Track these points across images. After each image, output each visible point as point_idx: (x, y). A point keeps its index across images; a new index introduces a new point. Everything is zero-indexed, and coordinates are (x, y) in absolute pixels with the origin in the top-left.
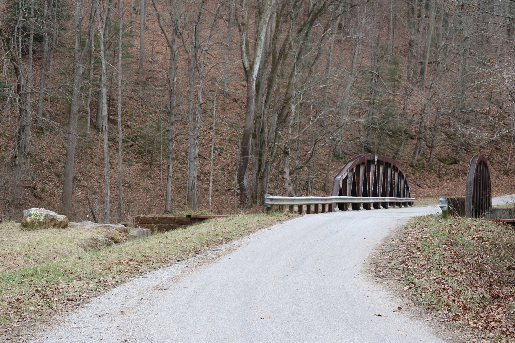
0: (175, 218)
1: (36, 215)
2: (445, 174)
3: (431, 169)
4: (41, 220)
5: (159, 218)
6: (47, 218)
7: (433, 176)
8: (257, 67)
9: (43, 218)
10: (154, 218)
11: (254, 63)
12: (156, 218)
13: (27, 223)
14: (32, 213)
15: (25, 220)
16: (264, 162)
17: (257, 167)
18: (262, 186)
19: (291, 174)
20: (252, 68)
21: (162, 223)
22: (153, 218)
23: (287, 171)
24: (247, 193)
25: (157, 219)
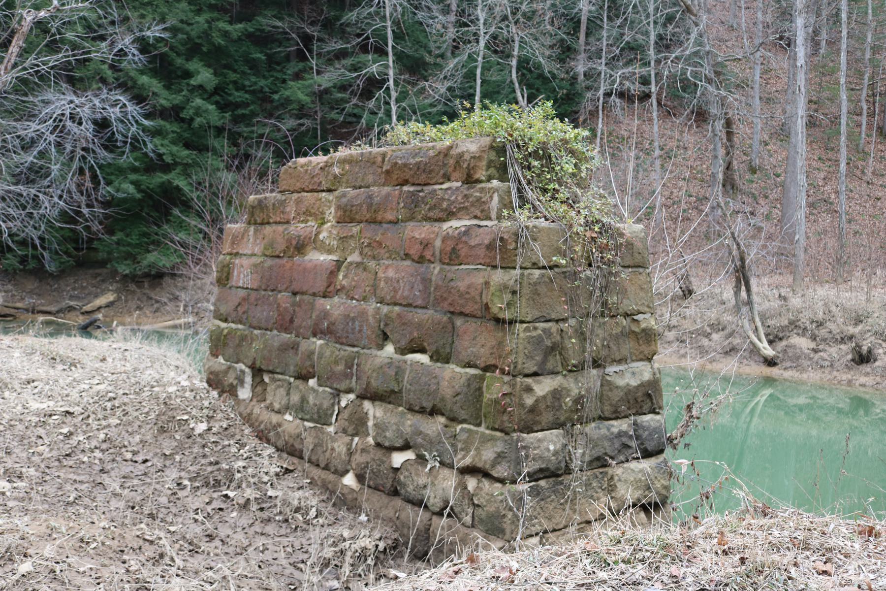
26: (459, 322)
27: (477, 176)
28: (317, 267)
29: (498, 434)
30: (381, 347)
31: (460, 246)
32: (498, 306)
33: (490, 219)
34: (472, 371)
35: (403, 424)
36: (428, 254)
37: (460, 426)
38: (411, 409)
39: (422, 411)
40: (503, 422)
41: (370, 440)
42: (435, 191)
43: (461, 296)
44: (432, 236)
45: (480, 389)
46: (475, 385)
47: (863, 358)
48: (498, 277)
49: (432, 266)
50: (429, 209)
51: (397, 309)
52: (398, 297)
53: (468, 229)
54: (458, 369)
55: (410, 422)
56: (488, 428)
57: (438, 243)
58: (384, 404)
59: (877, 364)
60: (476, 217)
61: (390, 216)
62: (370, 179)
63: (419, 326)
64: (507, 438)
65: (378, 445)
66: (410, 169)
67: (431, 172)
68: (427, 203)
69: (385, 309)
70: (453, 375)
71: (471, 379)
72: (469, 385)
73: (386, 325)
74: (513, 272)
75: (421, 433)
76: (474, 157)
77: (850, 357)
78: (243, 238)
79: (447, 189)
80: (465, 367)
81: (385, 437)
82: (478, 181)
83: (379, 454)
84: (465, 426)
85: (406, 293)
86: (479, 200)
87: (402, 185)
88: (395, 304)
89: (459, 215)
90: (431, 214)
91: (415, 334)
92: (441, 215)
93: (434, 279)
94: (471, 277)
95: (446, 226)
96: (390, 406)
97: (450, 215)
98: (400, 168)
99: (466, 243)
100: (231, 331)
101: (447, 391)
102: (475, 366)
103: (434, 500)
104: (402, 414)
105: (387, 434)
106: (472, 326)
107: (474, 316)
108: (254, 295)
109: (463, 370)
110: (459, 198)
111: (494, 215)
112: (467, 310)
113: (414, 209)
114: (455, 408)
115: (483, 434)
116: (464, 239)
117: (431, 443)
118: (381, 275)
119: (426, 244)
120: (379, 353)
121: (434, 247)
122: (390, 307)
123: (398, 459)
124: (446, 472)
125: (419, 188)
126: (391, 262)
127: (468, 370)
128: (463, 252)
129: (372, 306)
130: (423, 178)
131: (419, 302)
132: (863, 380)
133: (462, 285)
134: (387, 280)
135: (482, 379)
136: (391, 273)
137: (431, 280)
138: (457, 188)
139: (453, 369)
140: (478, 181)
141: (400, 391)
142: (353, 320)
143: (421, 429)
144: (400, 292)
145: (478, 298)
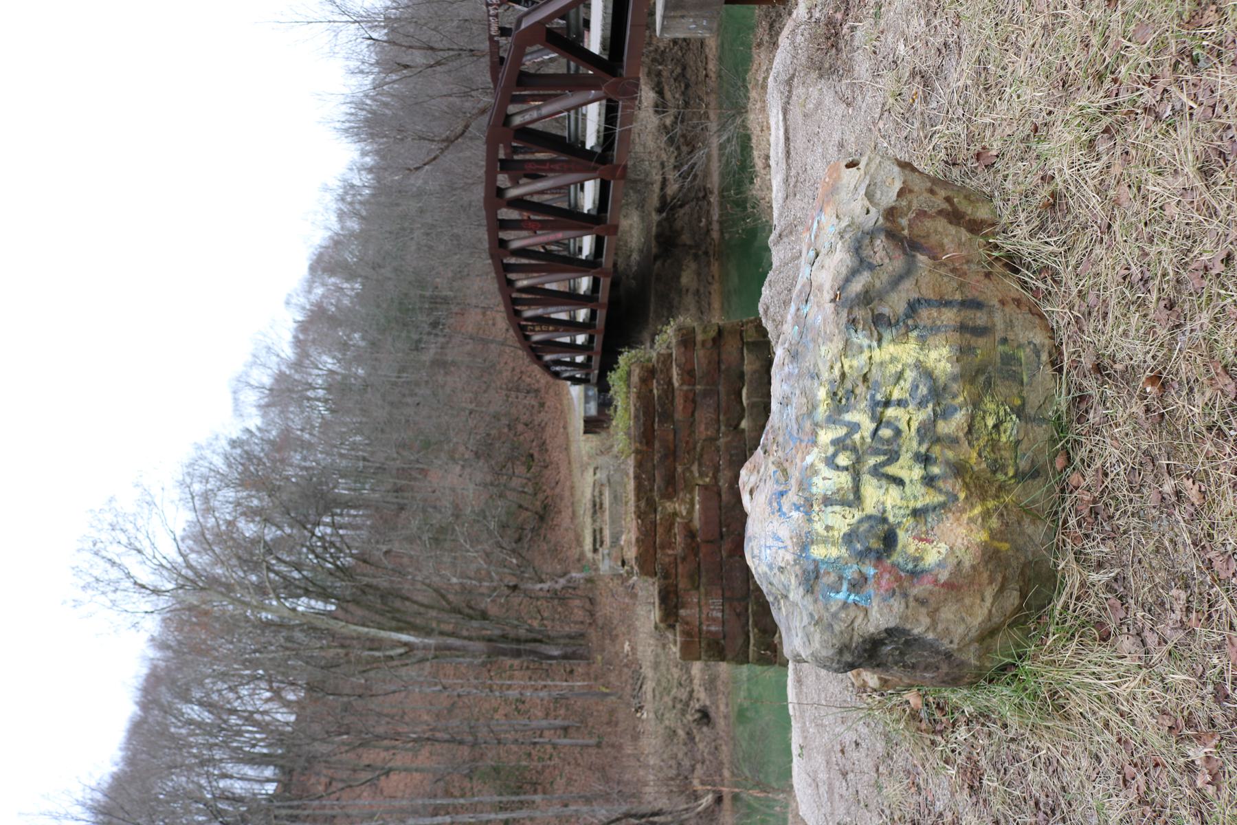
0: (637, 452)
1: (873, 456)
4: (940, 358)
5: (638, 499)
6: (896, 304)
7: (547, 472)
8: (404, 637)
9: (899, 353)
10: (640, 515)
11: (399, 642)
12: (638, 507)
13: (990, 556)
14: (840, 520)
15: (956, 585)
16: (531, 635)
17: (537, 644)
18: (563, 637)
19: (542, 581)
20: (406, 644)
21: (652, 490)
22: (639, 517)
23: (539, 586)
24: (569, 650)
25: (643, 504)
26: (723, 367)
28: (704, 509)
30: (743, 430)
32: (713, 334)
33: (671, 355)
36: (691, 395)
43: (710, 362)
47: (705, 716)
48: (700, 337)
51: (721, 417)
57: (685, 388)
59: (708, 703)
61: (671, 437)
62: (650, 464)
69: (723, 428)
77: (705, 729)
78: (687, 623)
85: (711, 410)
94: (701, 356)
95: (676, 384)
97: (670, 383)
100: (756, 624)
101: (757, 365)
106: (724, 357)
108: (728, 594)
113: (667, 416)
118: (703, 437)
129: (722, 441)
132: (722, 708)
134: (707, 429)
135: (748, 343)
136: (703, 427)
139: (747, 368)
142: (731, 456)
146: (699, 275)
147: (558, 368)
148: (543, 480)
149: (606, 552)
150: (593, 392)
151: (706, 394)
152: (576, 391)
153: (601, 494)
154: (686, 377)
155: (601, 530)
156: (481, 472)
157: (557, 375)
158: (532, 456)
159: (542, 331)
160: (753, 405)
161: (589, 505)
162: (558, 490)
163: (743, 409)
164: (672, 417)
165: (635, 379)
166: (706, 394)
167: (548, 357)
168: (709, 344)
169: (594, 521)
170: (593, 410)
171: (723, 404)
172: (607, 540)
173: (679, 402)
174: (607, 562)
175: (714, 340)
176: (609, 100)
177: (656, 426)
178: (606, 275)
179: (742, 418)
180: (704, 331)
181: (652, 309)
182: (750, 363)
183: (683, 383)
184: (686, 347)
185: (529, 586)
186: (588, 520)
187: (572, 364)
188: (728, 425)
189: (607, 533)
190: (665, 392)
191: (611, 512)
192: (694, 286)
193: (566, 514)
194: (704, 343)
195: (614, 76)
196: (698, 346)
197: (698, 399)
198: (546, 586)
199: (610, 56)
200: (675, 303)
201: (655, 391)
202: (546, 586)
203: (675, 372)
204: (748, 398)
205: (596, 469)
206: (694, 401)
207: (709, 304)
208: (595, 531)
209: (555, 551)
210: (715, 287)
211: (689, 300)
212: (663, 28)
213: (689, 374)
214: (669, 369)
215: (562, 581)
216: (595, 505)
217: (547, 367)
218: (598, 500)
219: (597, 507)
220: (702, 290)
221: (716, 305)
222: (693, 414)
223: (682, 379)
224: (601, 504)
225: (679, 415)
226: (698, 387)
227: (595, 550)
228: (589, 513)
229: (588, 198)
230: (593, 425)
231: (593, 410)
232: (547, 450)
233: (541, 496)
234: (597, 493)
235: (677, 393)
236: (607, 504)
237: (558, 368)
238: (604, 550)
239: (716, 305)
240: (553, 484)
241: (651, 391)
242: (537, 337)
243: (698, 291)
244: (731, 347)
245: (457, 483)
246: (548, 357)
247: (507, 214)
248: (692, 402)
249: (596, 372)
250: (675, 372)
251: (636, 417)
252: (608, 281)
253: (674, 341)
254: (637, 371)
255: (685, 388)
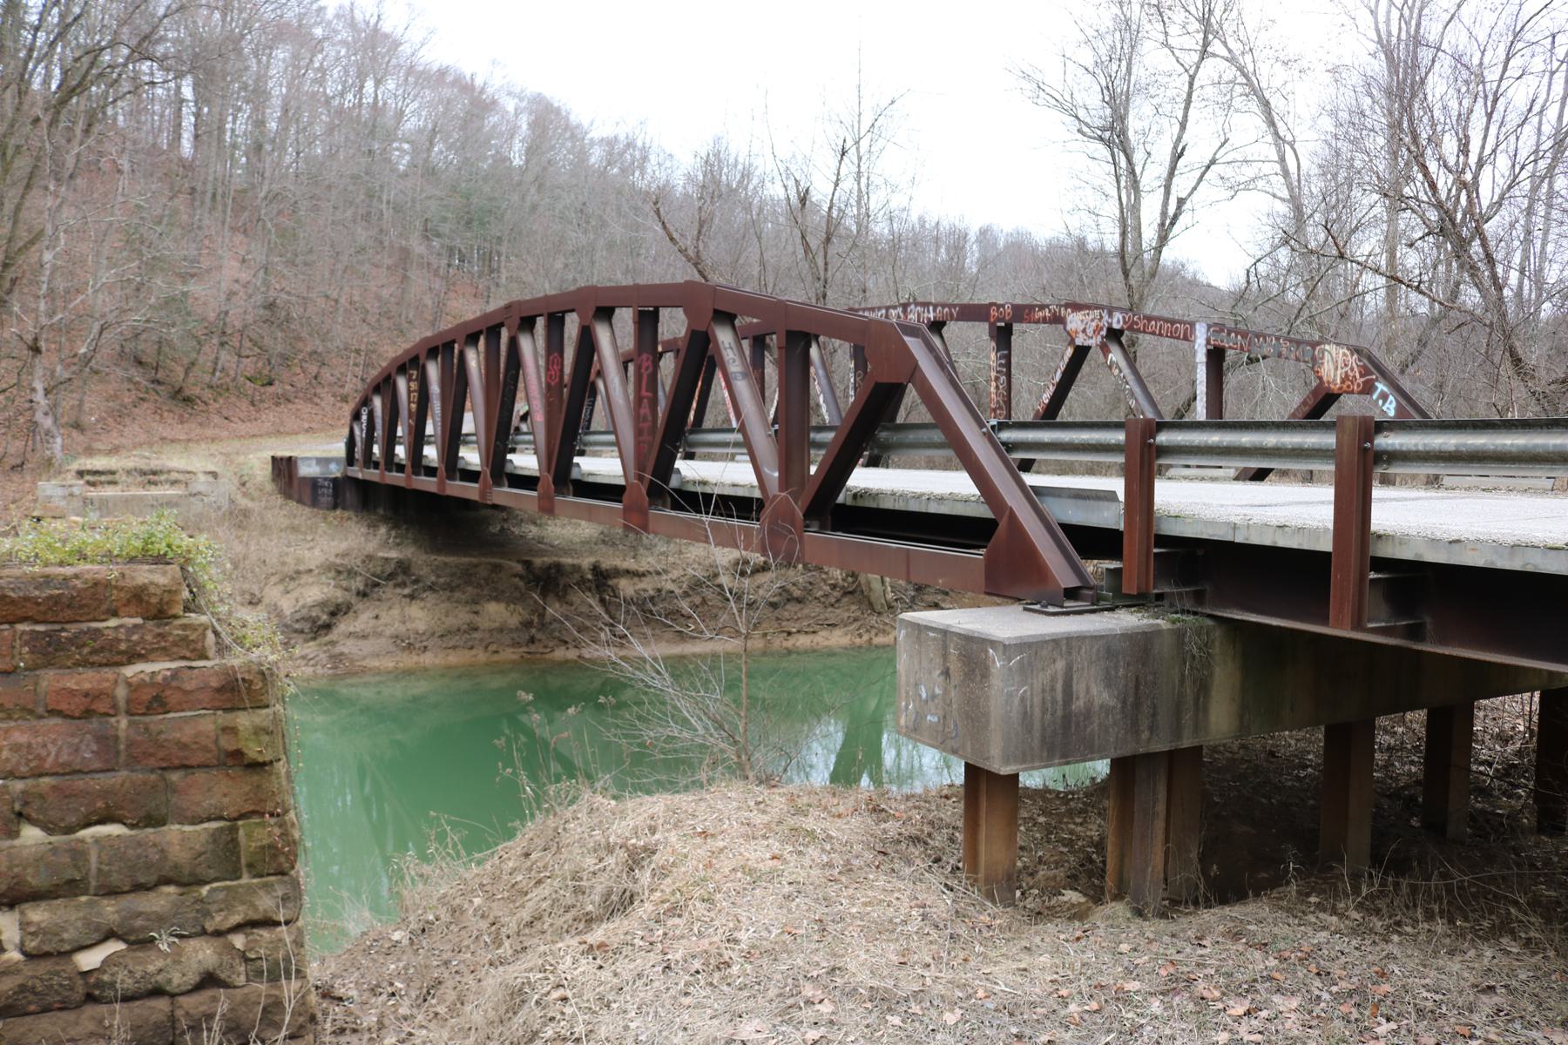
2: (262, 401)
3: (241, 394)
7: (244, 405)
19: (47, 392)
26: (175, 777)
27: (171, 612)
29: (272, 878)
30: (15, 834)
31: (168, 693)
32: (253, 751)
33: (207, 658)
34: (214, 825)
35: (99, 914)
36: (101, 707)
37: (207, 888)
38: (112, 892)
39: (138, 888)
40: (280, 864)
41: (14, 955)
42: (97, 630)
43: (185, 746)
44: (106, 685)
45: (234, 841)
46: (225, 838)
48: (244, 720)
49: (113, 720)
50: (91, 653)
51: (46, 780)
52: (47, 766)
53: (176, 673)
54: (188, 828)
55: (110, 911)
56: (255, 876)
57: (121, 693)
58: (43, 904)
60: (184, 658)
63: (105, 793)
64: (286, 878)
65: (30, 956)
66: (39, 604)
67: (82, 607)
68: (84, 645)
69: (18, 786)
70: (180, 839)
71: (215, 836)
72: (215, 841)
73: (26, 803)
74: (265, 711)
75: (140, 914)
76: (170, 591)
79: (116, 628)
80: (202, 822)
81: (62, 940)
82: (176, 617)
83: (43, 967)
84: (215, 885)
85: (64, 758)
86: (184, 639)
87: (11, 623)
88: (40, 775)
89: (151, 657)
90: (95, 658)
91: (100, 804)
92: (117, 658)
93: (122, 734)
94: (197, 725)
95: (129, 671)
96: (59, 901)
97: (133, 657)
98: (13, 602)
99: (179, 688)
102: (221, 818)
103: (178, 979)
104: (90, 904)
105: (65, 936)
106: (200, 776)
107: (207, 766)
109: (198, 828)
110: (149, 637)
111: (211, 653)
112: (193, 762)
113: (49, 652)
114: (198, 870)
115: (249, 886)
116: (174, 684)
117: (160, 920)
119: (97, 695)
120: (16, 842)
121: (114, 697)
122: (30, 782)
123: (89, 960)
124: (193, 943)
125: (57, 627)
126: (12, 724)
127: (206, 825)
128: (173, 697)
130: (68, 613)
131: (97, 765)
133: (186, 734)
135: (233, 830)
137: (117, 738)
138: (136, 626)
140: (176, 617)
141: (85, 879)
143: (140, 909)
144: (50, 760)
145: (212, 746)
146: (501, 630)
147: (364, 418)
148: (233, 399)
149: (76, 491)
150: (335, 471)
151: (107, 742)
152: (339, 449)
153: (174, 483)
154: (146, 695)
155: (114, 483)
156: (242, 312)
157: (356, 416)
158: (271, 384)
159: (409, 392)
160: (78, 854)
161: (155, 464)
162: (216, 419)
163: (70, 830)
164: (49, 664)
165: (144, 575)
166: (107, 742)
167: (377, 402)
168: (227, 743)
169: (129, 472)
170: (306, 470)
171: (80, 783)
172: (93, 493)
173: (87, 679)
174: (60, 492)
175: (238, 754)
176: (761, 503)
177: (21, 627)
178: (483, 493)
179: (48, 828)
180: (259, 731)
181: (451, 559)
182: (185, 839)
183: (134, 687)
184: (219, 690)
185: (39, 372)
186: (130, 463)
187: (369, 440)
188: (26, 798)
189: (109, 492)
190: (111, 646)
191: (141, 498)
192: (483, 623)
193: (179, 432)
194: (231, 730)
195: (807, 515)
196: (223, 718)
197: (94, 724)
198: (39, 397)
199: (843, 506)
200: (457, 595)
201: (113, 622)
202: (39, 397)
203: (161, 667)
204: (97, 840)
205: (214, 475)
206: (88, 714)
207: (454, 647)
208: (113, 473)
209: (120, 415)
210: (481, 656)
211: (462, 616)
212: (919, 629)
213: (156, 699)
214: (166, 653)
215: (48, 422)
216: (154, 473)
217: (366, 402)
218: (163, 478)
219: (151, 476)
220: (476, 635)
221: (453, 658)
222: (53, 713)
223: (142, 685)
224: (155, 483)
225: (50, 679)
226: (124, 722)
227: (81, 474)
228: (142, 464)
229: (601, 465)
230: (284, 468)
231: (306, 470)
232: (278, 404)
233: (207, 394)
234: (174, 476)
235: (108, 673)
236: (155, 491)
237: (364, 418)
238: (79, 486)
239: (453, 658)
240: (225, 413)
241: (115, 614)
242: (402, 383)
243: (476, 629)
244: (225, 792)
245: (226, 278)
246: (377, 402)
247: (572, 325)
248: (89, 709)
249: (360, 476)
250: (161, 667)
251: (47, 580)
252: (475, 496)
253: (236, 662)
254: (162, 580)
255: (121, 693)
